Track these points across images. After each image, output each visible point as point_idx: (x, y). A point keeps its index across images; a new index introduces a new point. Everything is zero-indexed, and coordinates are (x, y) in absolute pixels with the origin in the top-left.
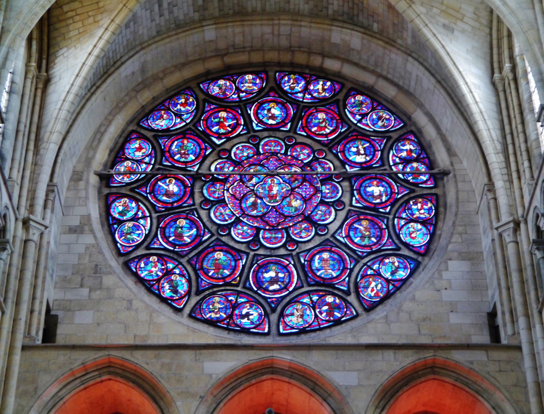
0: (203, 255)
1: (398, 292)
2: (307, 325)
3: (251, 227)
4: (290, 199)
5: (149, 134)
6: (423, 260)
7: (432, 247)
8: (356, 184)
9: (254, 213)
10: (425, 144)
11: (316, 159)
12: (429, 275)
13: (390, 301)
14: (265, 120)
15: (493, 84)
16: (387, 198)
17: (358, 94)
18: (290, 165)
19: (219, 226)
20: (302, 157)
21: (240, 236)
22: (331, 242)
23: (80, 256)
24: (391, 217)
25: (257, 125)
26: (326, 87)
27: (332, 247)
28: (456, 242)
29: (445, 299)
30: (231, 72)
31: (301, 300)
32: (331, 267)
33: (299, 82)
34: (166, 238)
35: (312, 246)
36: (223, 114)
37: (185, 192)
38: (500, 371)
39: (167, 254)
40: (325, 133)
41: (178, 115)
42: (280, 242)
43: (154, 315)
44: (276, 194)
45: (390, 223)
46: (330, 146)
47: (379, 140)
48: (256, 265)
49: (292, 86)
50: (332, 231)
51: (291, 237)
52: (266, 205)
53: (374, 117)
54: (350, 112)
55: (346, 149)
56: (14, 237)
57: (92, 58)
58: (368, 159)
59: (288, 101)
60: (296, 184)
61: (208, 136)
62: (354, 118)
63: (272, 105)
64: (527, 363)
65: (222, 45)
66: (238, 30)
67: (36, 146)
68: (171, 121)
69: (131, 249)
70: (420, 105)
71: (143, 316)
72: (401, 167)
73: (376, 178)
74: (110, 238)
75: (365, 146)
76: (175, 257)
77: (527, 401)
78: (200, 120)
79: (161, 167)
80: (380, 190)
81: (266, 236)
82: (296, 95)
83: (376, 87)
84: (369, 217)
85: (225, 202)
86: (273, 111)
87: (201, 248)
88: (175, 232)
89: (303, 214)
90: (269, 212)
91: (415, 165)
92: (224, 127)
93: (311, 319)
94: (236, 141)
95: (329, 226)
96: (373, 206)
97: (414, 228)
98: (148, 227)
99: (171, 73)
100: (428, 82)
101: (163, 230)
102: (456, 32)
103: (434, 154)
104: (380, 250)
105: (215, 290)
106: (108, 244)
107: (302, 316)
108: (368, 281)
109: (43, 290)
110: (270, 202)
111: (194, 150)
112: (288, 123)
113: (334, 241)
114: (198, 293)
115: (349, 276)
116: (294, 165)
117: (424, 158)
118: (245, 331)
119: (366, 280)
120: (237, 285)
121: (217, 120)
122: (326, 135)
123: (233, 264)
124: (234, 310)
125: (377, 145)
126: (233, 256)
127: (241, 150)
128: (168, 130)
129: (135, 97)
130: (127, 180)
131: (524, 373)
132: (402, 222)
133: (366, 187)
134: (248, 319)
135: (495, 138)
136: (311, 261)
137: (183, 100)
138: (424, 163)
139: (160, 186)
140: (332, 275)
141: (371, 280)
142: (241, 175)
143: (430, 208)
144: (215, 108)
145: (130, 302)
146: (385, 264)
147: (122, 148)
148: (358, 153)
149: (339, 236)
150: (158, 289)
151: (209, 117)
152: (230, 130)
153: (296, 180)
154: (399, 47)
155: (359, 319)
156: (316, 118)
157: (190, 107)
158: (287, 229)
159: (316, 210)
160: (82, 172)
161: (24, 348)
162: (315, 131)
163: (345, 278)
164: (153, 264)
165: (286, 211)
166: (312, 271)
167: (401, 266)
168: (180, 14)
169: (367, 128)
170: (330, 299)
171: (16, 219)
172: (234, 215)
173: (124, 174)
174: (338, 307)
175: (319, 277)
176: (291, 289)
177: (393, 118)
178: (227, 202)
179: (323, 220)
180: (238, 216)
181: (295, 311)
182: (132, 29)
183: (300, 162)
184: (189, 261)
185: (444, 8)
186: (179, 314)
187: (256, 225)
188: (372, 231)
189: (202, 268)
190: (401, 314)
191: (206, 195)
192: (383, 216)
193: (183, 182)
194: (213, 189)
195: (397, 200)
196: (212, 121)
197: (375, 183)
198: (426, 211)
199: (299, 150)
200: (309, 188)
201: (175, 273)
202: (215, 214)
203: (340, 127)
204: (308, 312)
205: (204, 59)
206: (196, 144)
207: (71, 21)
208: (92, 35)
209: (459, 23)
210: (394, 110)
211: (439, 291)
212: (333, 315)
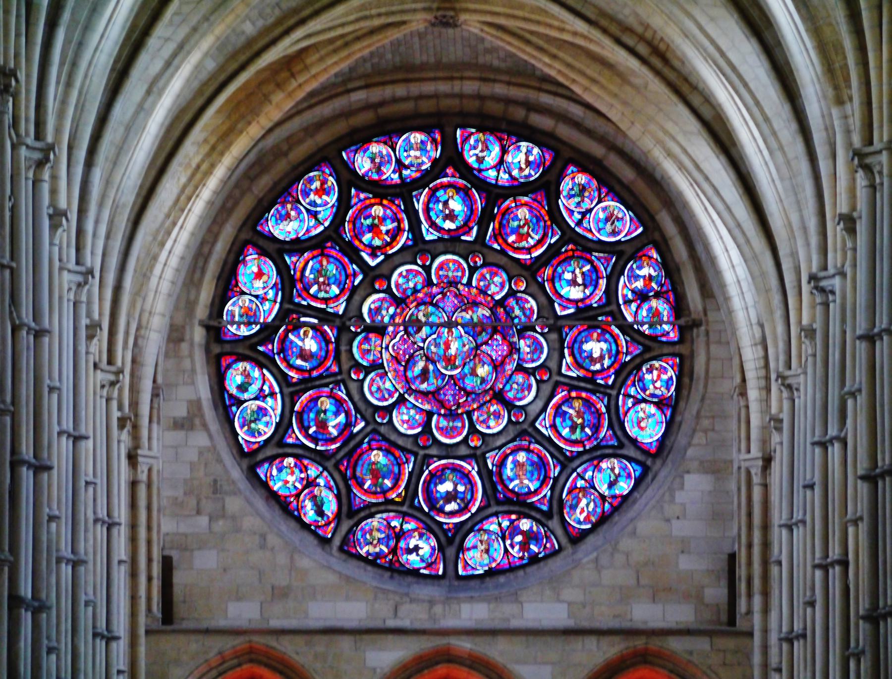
0: (355, 457)
1: (616, 514)
3: (421, 411)
4: (475, 364)
5: (271, 247)
6: (654, 463)
7: (668, 443)
9: (424, 387)
11: (512, 293)
13: (605, 527)
14: (439, 221)
16: (610, 362)
17: (579, 172)
18: (475, 304)
19: (377, 408)
20: (493, 289)
21: (405, 426)
22: (530, 435)
23: (192, 466)
25: (428, 230)
26: (531, 158)
27: (530, 442)
28: (699, 445)
29: (675, 532)
31: (486, 527)
32: (529, 475)
33: (491, 147)
34: (304, 429)
36: (378, 211)
37: (327, 351)
38: (725, 664)
41: (314, 215)
42: (460, 434)
43: (296, 557)
44: (455, 356)
45: (613, 403)
47: (605, 258)
49: (481, 155)
50: (531, 418)
54: (566, 208)
55: (557, 275)
58: (588, 292)
60: (484, 336)
61: (357, 251)
63: (451, 194)
64: (757, 659)
69: (256, 446)
71: (282, 559)
72: (634, 306)
74: (228, 429)
75: (585, 269)
79: (291, 307)
80: (602, 350)
81: (441, 426)
82: (485, 174)
83: (605, 163)
84: (584, 395)
85: (384, 368)
87: (352, 444)
88: (316, 418)
89: (492, 388)
91: (654, 303)
93: (499, 555)
94: (397, 260)
95: (529, 409)
96: (590, 375)
97: (644, 412)
98: (279, 411)
99: (300, 142)
101: (300, 415)
103: (683, 283)
105: (373, 510)
106: (226, 438)
110: (446, 369)
111: (338, 276)
112: (472, 228)
113: (534, 433)
114: (351, 514)
115: (552, 489)
116: (481, 304)
117: (667, 292)
119: (574, 496)
120: (401, 504)
121: (369, 222)
122: (528, 250)
123: (396, 469)
124: (398, 542)
125: (602, 268)
126: (396, 458)
127: (405, 277)
128: (297, 240)
129: (249, 189)
131: (751, 667)
132: (630, 402)
133: (582, 343)
134: (418, 555)
135: (754, 320)
136: (502, 464)
137: (316, 185)
138: (668, 301)
139: (292, 342)
140: (529, 488)
144: (366, 198)
145: (263, 537)
146: (600, 470)
148: (573, 283)
149: (540, 424)
150: (298, 510)
153: (484, 330)
159: (511, 382)
160: (183, 327)
161: (148, 632)
162: (513, 242)
164: (289, 471)
165: (470, 383)
166: (502, 482)
167: (623, 473)
169: (589, 236)
170: (525, 524)
172: (396, 390)
175: (512, 491)
176: (474, 510)
178: (387, 369)
179: (520, 399)
180: (402, 392)
181: (479, 543)
183: (489, 298)
184: (337, 466)
186: (327, 547)
187: (427, 407)
189: (354, 476)
191: (357, 356)
193: (324, 334)
194: (366, 346)
195: (626, 363)
196: (362, 224)
199: (488, 276)
201: (318, 485)
203: (550, 235)
204: (496, 545)
210: (631, 201)
211: (668, 520)
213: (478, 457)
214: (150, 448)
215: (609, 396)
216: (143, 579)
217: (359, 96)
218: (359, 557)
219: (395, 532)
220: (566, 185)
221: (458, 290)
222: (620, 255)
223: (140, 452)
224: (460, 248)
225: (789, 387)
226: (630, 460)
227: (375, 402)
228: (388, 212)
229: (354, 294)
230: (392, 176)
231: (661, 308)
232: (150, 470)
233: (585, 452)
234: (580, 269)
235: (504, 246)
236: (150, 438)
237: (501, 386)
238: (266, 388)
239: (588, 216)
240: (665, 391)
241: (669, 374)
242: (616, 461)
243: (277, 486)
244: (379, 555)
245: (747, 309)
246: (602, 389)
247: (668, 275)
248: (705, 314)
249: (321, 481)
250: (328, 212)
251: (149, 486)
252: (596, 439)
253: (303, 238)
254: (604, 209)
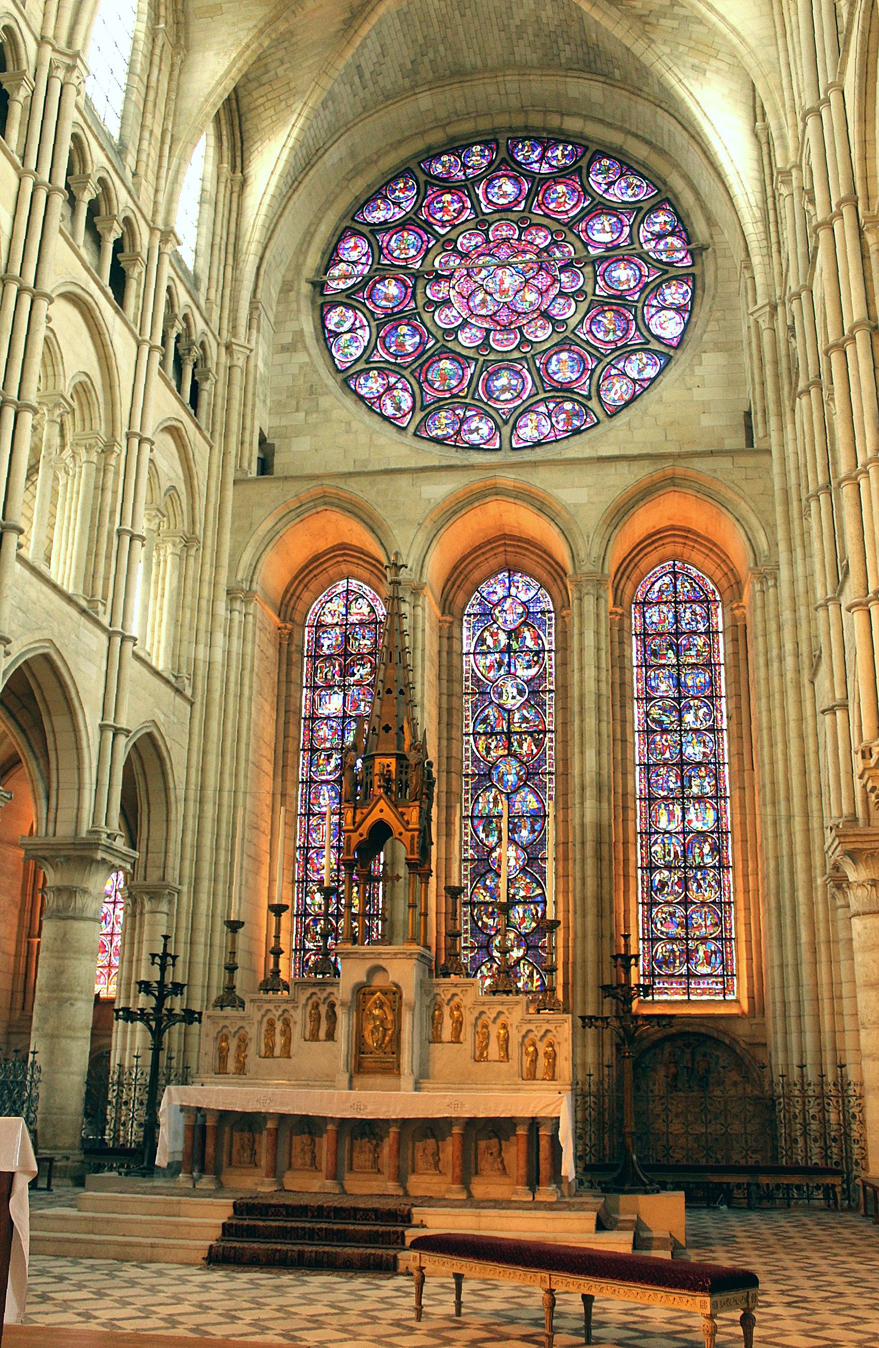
0: (427, 365)
5: (365, 230)
7: (686, 337)
9: (483, 312)
10: (681, 214)
11: (554, 243)
12: (679, 372)
13: (635, 403)
14: (495, 200)
15: (756, 136)
18: (525, 252)
20: (538, 241)
24: (640, 305)
30: (456, 145)
34: (386, 349)
36: (447, 197)
39: (388, 366)
41: (397, 204)
43: (374, 437)
45: (639, 312)
46: (570, 225)
50: (571, 328)
53: (623, 184)
56: (217, 364)
57: (286, 151)
58: (615, 237)
59: (522, 174)
61: (430, 225)
64: (776, 469)
65: (442, 113)
66: (457, 94)
67: (235, 259)
69: (348, 365)
70: (676, 166)
71: (363, 439)
73: (623, 260)
76: (397, 369)
77: (774, 510)
78: (421, 206)
84: (614, 308)
86: (504, 188)
91: (670, 239)
94: (462, 228)
98: (367, 339)
99: (387, 153)
100: (681, 137)
102: (708, 74)
104: (626, 345)
107: (537, 427)
109: (253, 419)
114: (423, 408)
115: (590, 378)
118: (475, 447)
120: (465, 397)
121: (440, 205)
122: (566, 212)
123: (460, 372)
128: (385, 222)
131: (772, 480)
135: (753, 204)
142: (467, 269)
145: (349, 424)
147: (336, 249)
148: (603, 230)
151: (431, 203)
154: (645, 96)
155: (600, 427)
156: (555, 192)
158: (519, 328)
161: (235, 482)
168: (386, 82)
169: (614, 199)
170: (568, 406)
171: (218, 344)
173: (339, 278)
174: (577, 414)
176: (524, 397)
182: (332, 109)
185: (692, 44)
187: (486, 326)
188: (618, 323)
189: (426, 380)
190: (646, 418)
192: (628, 306)
193: (403, 282)
195: (647, 284)
197: (622, 265)
204: (543, 422)
205: (423, 133)
207: (261, 109)
208: (285, 123)
209: (713, 62)
210: (646, 174)
212: (571, 424)
224: (511, 216)
233: (618, 349)
243: (363, 392)
247: (680, 219)
248: (712, 238)
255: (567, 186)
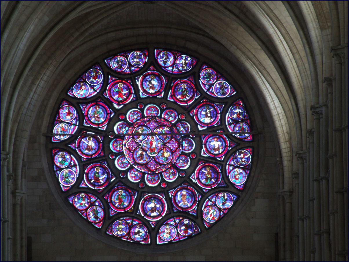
2: (172, 239)
4: (163, 152)
5: (74, 102)
8: (204, 140)
9: (141, 162)
11: (179, 121)
14: (147, 89)
16: (223, 150)
17: (208, 68)
18: (164, 126)
21: (133, 179)
22: (188, 182)
26: (187, 62)
27: (188, 186)
31: (169, 223)
32: (187, 200)
33: (170, 57)
34: (89, 181)
35: (176, 185)
36: (120, 85)
37: (99, 147)
40: (186, 100)
41: (92, 87)
44: (155, 148)
45: (224, 168)
46: (188, 109)
48: (143, 199)
49: (165, 60)
51: (164, 179)
52: (149, 156)
54: (202, 83)
55: (199, 112)
58: (212, 120)
60: (167, 140)
61: (111, 103)
62: (205, 87)
63: (152, 77)
68: (87, 91)
72: (232, 126)
79: (83, 127)
80: (219, 144)
82: (167, 69)
84: (211, 165)
86: (153, 82)
87: (110, 187)
89: (171, 162)
90: (150, 161)
92: (121, 95)
93: (175, 235)
96: (213, 156)
97: (238, 172)
98: (78, 173)
105: (119, 216)
107: (170, 233)
108: (208, 209)
110: (151, 154)
112: (162, 93)
121: (116, 90)
122: (186, 102)
124: (130, 230)
126: (129, 194)
127: (133, 114)
128: (85, 98)
130: (63, 138)
132: (231, 168)
133: (210, 142)
134: (139, 235)
135: (285, 132)
136: (175, 196)
137: (94, 74)
138: (247, 124)
139: (84, 142)
140: (187, 205)
141: (210, 208)
143: (249, 157)
144: (115, 80)
146: (219, 198)
147: (58, 113)
148: (206, 116)
150: (86, 216)
152: (125, 98)
156: (181, 88)
157: (99, 79)
158: (161, 173)
162: (180, 98)
163: (195, 207)
164: (82, 199)
165: (161, 160)
167: (228, 199)
170: (186, 222)
172: (129, 163)
175: (180, 207)
176: (163, 215)
177: (230, 88)
178: (125, 154)
179: (183, 167)
180: (132, 164)
181: (166, 229)
187: (142, 170)
189: (111, 201)
191: (112, 149)
196: (114, 91)
198: (246, 159)
200: (175, 143)
201: (95, 205)
202: (118, 161)
203: (196, 95)
204: (173, 231)
206: (104, 110)
213: (165, 192)
214: (21, 189)
215: (222, 165)
216: (19, 246)
217: (111, 35)
218: (113, 236)
219: (129, 225)
220: (202, 74)
221: (155, 119)
222: (226, 103)
223: (17, 191)
225: (302, 158)
226: (232, 193)
227: (120, 169)
228: (125, 86)
229: (111, 122)
230: (127, 70)
231: (244, 127)
232: (21, 199)
233: (212, 189)
234: (209, 110)
235: (176, 100)
236: (21, 185)
237: (175, 161)
238: (72, 163)
239: (212, 87)
240: (246, 163)
241: (248, 155)
242: (225, 194)
243: (77, 206)
244: (122, 236)
245: (282, 126)
246: (219, 162)
249: (97, 204)
250: (99, 86)
251: (21, 206)
252: (217, 184)
253: (88, 97)
254: (219, 84)
255: (187, 84)
